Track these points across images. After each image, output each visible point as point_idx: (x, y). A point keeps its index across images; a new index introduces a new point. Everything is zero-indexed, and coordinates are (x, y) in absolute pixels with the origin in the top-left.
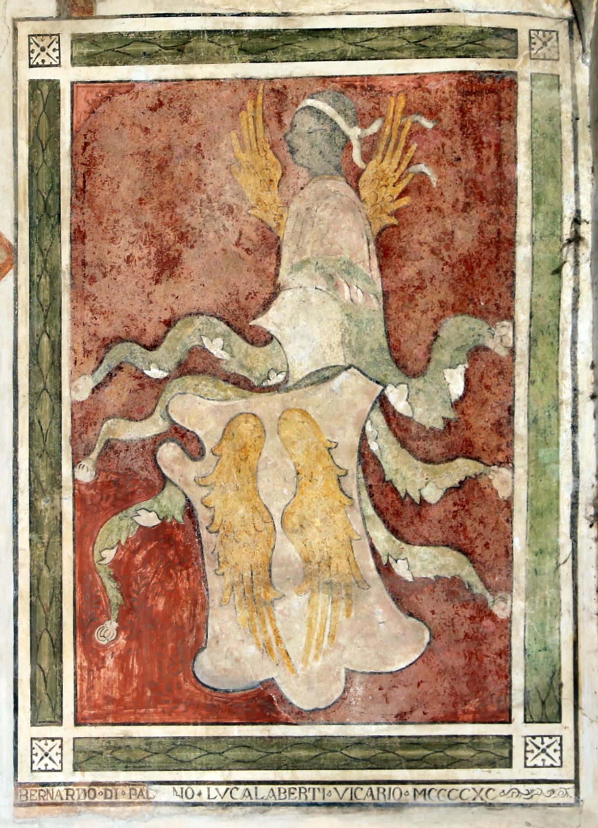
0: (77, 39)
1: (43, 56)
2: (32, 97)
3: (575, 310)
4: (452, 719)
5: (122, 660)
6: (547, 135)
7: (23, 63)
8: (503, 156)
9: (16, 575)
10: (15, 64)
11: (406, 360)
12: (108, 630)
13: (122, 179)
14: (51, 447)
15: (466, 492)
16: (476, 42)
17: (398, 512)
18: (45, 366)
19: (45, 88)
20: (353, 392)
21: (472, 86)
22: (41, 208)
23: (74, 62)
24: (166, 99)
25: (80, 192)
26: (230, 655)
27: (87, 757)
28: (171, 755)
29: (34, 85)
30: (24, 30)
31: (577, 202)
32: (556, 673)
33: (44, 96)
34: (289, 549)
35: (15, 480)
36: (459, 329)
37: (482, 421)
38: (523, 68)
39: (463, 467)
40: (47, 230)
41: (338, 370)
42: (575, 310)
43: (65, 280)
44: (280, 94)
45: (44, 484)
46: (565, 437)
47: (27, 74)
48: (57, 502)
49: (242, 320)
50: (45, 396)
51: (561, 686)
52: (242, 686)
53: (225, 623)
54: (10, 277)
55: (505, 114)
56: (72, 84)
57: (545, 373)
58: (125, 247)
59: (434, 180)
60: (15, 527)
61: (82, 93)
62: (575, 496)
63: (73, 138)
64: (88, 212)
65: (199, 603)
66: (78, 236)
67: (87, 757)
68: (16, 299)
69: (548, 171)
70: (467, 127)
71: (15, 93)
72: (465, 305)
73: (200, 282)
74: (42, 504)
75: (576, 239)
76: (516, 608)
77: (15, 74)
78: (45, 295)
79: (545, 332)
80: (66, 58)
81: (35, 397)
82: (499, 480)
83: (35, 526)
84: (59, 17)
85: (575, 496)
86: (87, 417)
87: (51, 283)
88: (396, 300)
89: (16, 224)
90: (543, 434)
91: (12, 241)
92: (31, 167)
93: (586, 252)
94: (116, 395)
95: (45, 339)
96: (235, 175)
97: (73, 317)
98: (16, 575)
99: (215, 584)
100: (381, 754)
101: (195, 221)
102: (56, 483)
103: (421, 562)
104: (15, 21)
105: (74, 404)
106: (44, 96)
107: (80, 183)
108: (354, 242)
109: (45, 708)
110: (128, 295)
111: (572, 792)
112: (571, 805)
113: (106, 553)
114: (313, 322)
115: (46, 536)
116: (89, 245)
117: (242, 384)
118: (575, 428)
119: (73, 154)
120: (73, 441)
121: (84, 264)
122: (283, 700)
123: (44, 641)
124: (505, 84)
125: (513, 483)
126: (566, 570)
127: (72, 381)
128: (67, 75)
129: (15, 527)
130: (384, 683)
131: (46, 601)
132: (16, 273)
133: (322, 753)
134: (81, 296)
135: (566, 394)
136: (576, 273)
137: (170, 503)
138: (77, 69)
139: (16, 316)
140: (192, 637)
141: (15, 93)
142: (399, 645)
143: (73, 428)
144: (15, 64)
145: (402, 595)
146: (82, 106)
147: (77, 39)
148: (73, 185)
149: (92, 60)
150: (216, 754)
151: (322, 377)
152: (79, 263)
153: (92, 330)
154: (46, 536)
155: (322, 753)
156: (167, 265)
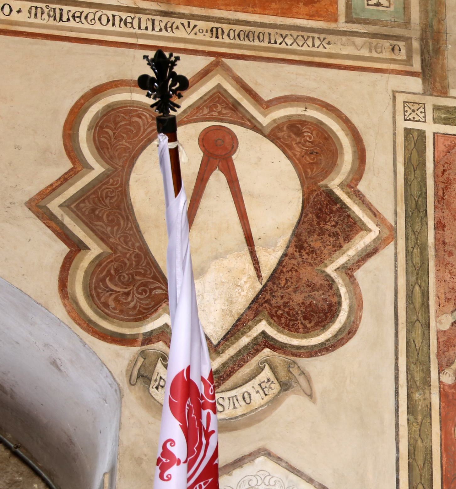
0: (437, 108)
1: (414, 115)
2: (406, 138)
7: (400, 118)
9: (397, 443)
10: (394, 117)
14: (422, 358)
18: (418, 304)
19: (416, 134)
22: (414, 206)
23: (435, 121)
25: (440, 199)
29: (408, 131)
30: (400, 98)
33: (415, 141)
35: (397, 378)
40: (417, 220)
43: (431, 252)
45: (418, 382)
47: (402, 125)
48: (427, 395)
50: (418, 325)
54: (391, 246)
56: (434, 134)
60: (397, 410)
61: (441, 140)
63: (435, 166)
64: (447, 212)
66: (440, 226)
68: (396, 260)
71: (395, 134)
74: (417, 396)
77: (394, 123)
78: (417, 260)
80: (429, 117)
81: (410, 326)
83: (411, 410)
84: (424, 94)
87: (421, 253)
89: (396, 214)
91: (393, 224)
92: (406, 180)
95: (417, 288)
97: (437, 276)
98: (397, 443)
102: (427, 383)
104: (394, 92)
105: (438, 332)
107: (441, 193)
115: (420, 418)
116: (447, 232)
119: (435, 176)
120: (438, 355)
121: (444, 243)
127: (437, 317)
128: (430, 128)
129: (397, 410)
131: (420, 463)
132: (396, 244)
134: (442, 263)
138: (437, 125)
139: (396, 271)
141: (395, 134)
143: (439, 347)
144: (394, 117)
146: (441, 147)
147: (437, 108)
148: (436, 194)
149: (447, 122)
152: (441, 243)
153: (451, 285)
154: (420, 418)
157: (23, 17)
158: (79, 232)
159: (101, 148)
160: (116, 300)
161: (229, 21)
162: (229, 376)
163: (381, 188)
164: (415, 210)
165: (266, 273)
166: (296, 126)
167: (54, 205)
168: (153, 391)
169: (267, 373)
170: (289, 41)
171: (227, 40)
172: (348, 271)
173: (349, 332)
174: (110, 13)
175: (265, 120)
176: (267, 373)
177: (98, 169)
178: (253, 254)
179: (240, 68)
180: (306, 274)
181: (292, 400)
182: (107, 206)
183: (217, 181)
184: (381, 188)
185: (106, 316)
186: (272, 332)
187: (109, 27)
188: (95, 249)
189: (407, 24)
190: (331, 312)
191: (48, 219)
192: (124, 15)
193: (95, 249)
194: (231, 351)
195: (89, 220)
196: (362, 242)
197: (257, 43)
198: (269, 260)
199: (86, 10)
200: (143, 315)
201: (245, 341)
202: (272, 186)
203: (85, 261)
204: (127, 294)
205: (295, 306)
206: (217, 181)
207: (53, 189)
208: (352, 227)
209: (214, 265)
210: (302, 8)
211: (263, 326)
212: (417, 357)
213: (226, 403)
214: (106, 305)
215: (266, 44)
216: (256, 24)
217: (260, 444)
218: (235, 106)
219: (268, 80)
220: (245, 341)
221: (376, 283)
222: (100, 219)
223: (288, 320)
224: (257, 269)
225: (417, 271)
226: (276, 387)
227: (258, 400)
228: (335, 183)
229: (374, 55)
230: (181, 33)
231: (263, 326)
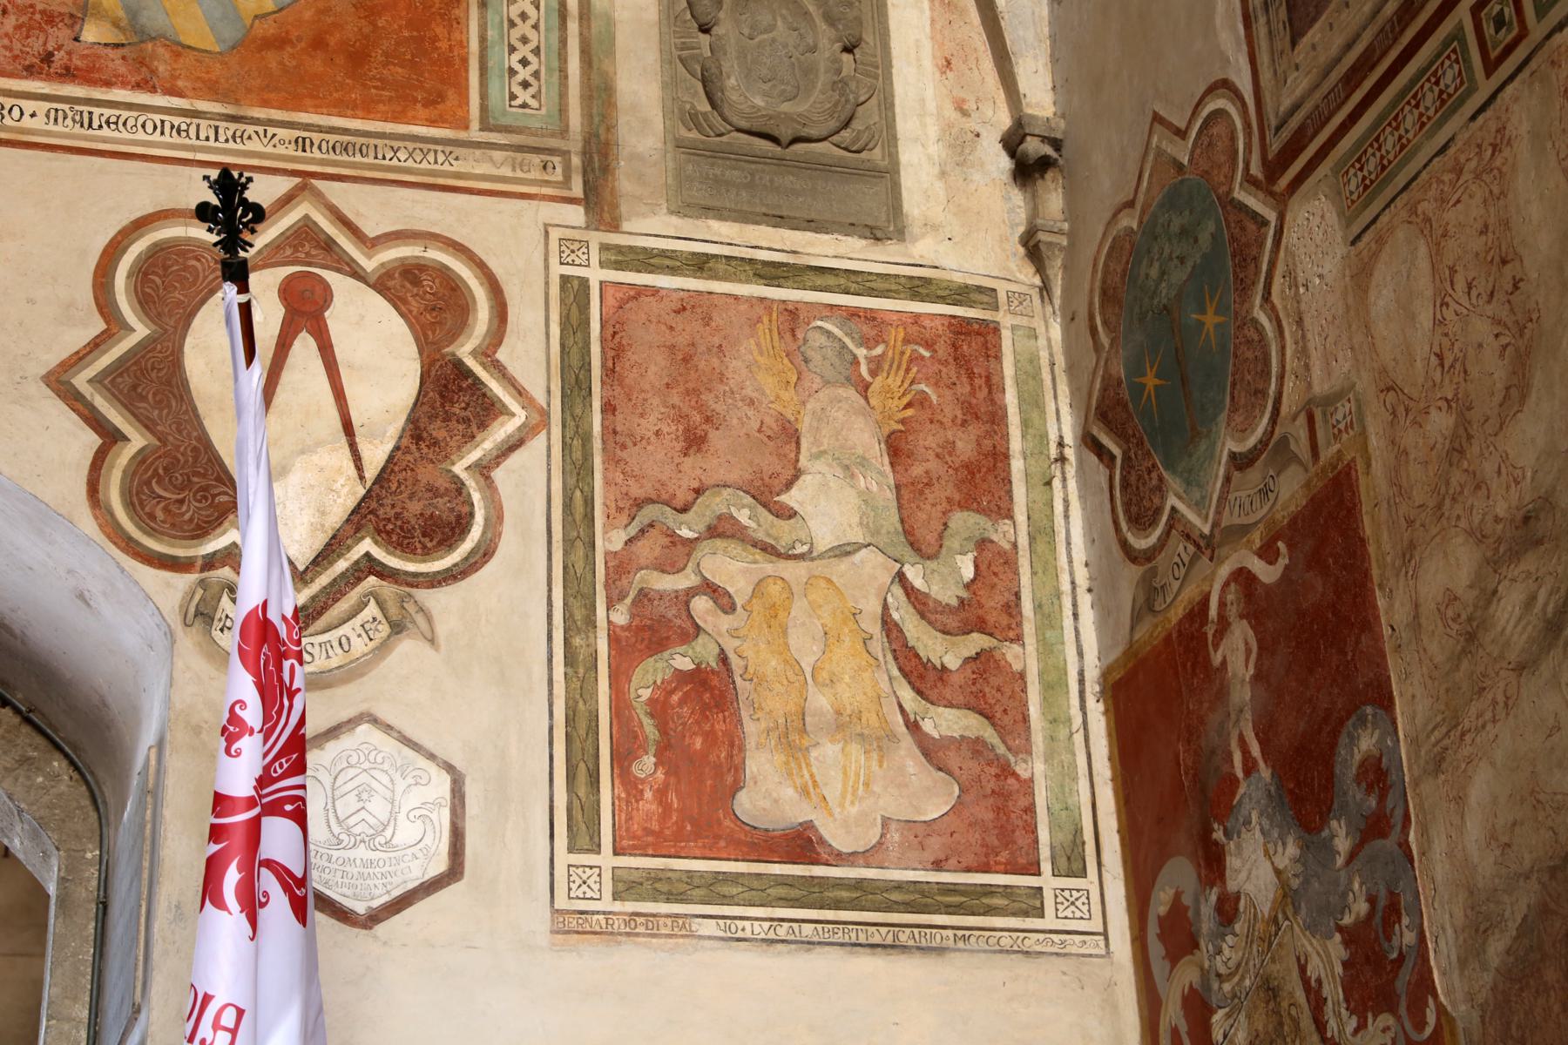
0: (604, 248)
1: (573, 256)
2: (563, 288)
3: (1067, 517)
4: (986, 869)
5: (661, 794)
6: (1029, 374)
7: (554, 261)
8: (993, 386)
9: (551, 705)
10: (546, 260)
11: (921, 544)
12: (646, 765)
13: (650, 367)
14: (585, 590)
15: (982, 662)
16: (962, 294)
17: (922, 676)
18: (578, 517)
19: (576, 283)
20: (872, 568)
21: (961, 328)
22: (573, 381)
23: (602, 265)
24: (686, 305)
25: (609, 372)
26: (768, 794)
27: (626, 887)
28: (713, 889)
29: (565, 279)
30: (555, 234)
31: (1060, 429)
32: (1078, 831)
33: (574, 291)
34: (820, 701)
35: (550, 616)
36: (965, 522)
37: (992, 603)
38: (1005, 320)
39: (977, 642)
40: (578, 400)
41: (860, 546)
42: (1067, 517)
43: (597, 444)
44: (792, 313)
45: (578, 622)
46: (1068, 622)
47: (557, 270)
48: (592, 640)
49: (767, 495)
50: (579, 543)
51: (1084, 843)
52: (782, 825)
53: (761, 764)
54: (543, 435)
55: (992, 352)
56: (601, 283)
57: (1045, 567)
58: (653, 421)
59: (934, 398)
60: (550, 660)
61: (610, 291)
62: (1081, 673)
63: (602, 327)
64: (618, 389)
65: (736, 745)
66: (609, 408)
67: (626, 887)
68: (549, 456)
69: (1032, 403)
70: (959, 359)
71: (547, 283)
72: (969, 502)
73: (725, 459)
74: (577, 641)
75: (1062, 459)
76: (1036, 768)
77: (547, 267)
78: (577, 455)
79: (1042, 532)
80: (595, 260)
81: (568, 544)
82: (1011, 652)
83: (570, 660)
84: (587, 228)
85: (1081, 673)
86: (620, 567)
87: (583, 445)
88: (908, 493)
89: (549, 392)
90: (1048, 618)
92: (563, 346)
93: (1071, 471)
94: (648, 549)
95: (578, 493)
96: (754, 375)
97: (605, 477)
98: (551, 705)
99: (750, 727)
100: (920, 899)
101: (720, 408)
102: (591, 622)
103: (945, 722)
104: (546, 225)
105: (607, 553)
106: (574, 291)
107: (610, 364)
108: (866, 440)
109: (583, 834)
110: (657, 462)
111: (1102, 944)
112: (1102, 956)
113: (642, 690)
114: (835, 502)
115: (581, 671)
116: (619, 417)
117: (769, 550)
118: (1076, 616)
119: (603, 340)
120: (607, 586)
121: (615, 432)
122: (822, 841)
123: (581, 769)
124: (988, 332)
125: (1024, 657)
126: (1079, 738)
127: (605, 533)
128: (596, 275)
129: (550, 660)
130: (919, 831)
131: (582, 732)
132: (549, 433)
133: (862, 895)
134: (611, 460)
135: (1066, 586)
136: (1065, 487)
137: (704, 651)
138: (605, 271)
139: (549, 470)
140: (731, 778)
141: (547, 283)
142: (934, 799)
143: (607, 574)
144: (546, 260)
145: (931, 750)
146: (610, 301)
147: (604, 248)
148: (603, 366)
149: (619, 266)
150: (759, 892)
151: (844, 551)
152: (610, 432)
153: (624, 490)
154: (581, 671)
155: (862, 895)
156: (694, 442)
157: (38, 123)
158: (115, 416)
159: (146, 302)
160: (166, 510)
161: (320, 129)
162: (320, 614)
163: (529, 356)
164: (575, 386)
165: (371, 473)
166: (412, 272)
167: (81, 381)
168: (216, 634)
169: (372, 610)
170: (402, 155)
171: (317, 154)
172: (484, 470)
173: (484, 553)
174: (157, 118)
175: (369, 264)
176: (372, 610)
177: (141, 330)
178: (353, 447)
179: (335, 192)
180: (426, 473)
181: (408, 648)
182: (153, 382)
183: (304, 347)
184: (529, 356)
185: (152, 532)
186: (379, 554)
187: (157, 137)
188: (137, 440)
189: (564, 132)
190: (460, 526)
191: (73, 398)
192: (177, 121)
193: (137, 440)
194: (324, 580)
195: (129, 401)
196: (502, 430)
197: (358, 158)
198: (375, 455)
199: (125, 114)
200: (202, 530)
201: (342, 565)
202: (379, 355)
203: (123, 457)
204: (181, 502)
205: (411, 517)
206: (304, 347)
207: (79, 359)
208: (489, 410)
209: (299, 463)
210: (422, 112)
211: (367, 546)
212: (577, 588)
213: (316, 651)
214: (152, 516)
215: (370, 160)
216: (357, 133)
217: (363, 707)
218: (329, 245)
219: (374, 209)
220: (342, 565)
221: (521, 487)
222: (143, 398)
223: (401, 538)
224: (359, 468)
225: (578, 470)
226: (385, 629)
227: (360, 646)
228: (465, 350)
229: (519, 174)
230: (255, 145)
231: (367, 546)
